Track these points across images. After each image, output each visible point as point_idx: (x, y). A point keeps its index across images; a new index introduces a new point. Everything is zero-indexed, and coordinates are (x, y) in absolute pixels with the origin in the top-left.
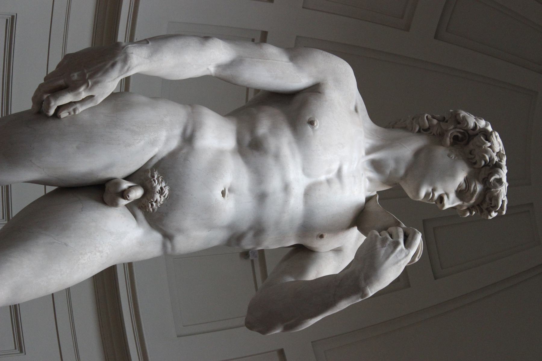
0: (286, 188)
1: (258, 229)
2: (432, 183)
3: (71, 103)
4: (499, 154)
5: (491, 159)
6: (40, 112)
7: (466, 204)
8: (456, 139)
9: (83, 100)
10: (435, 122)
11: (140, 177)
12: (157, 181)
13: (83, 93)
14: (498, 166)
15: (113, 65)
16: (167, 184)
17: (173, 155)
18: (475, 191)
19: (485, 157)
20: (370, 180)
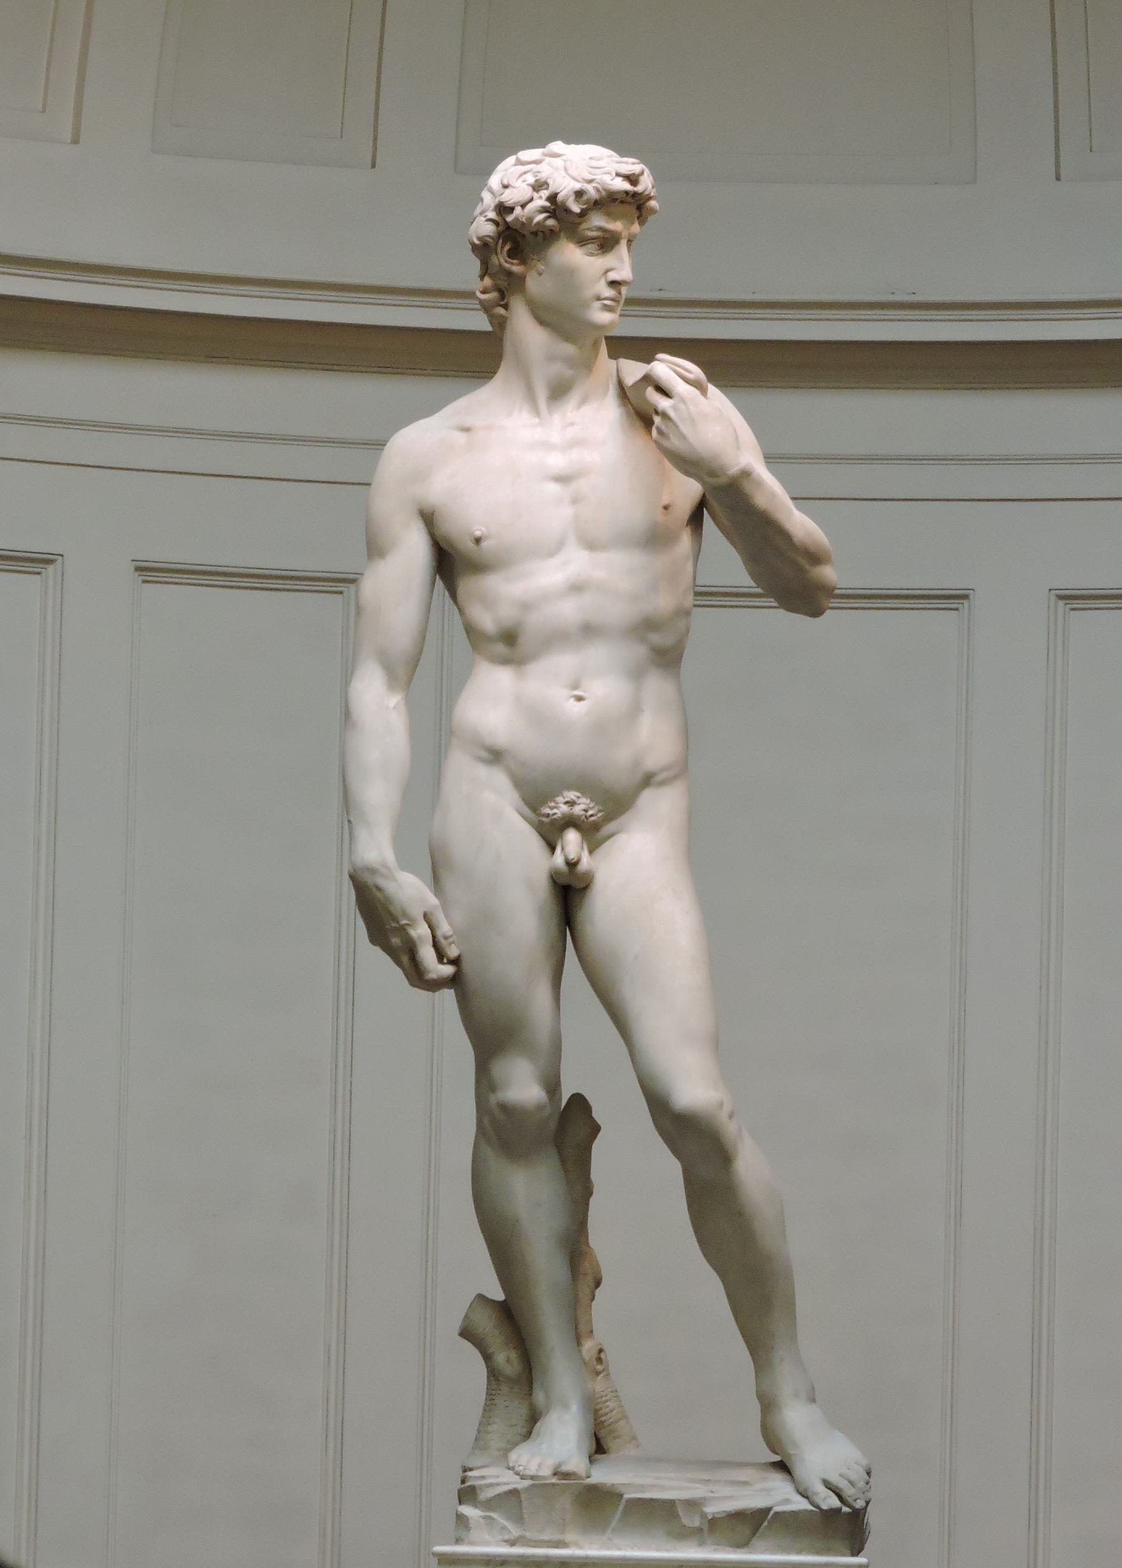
0: (576, 588)
1: (644, 627)
2: (586, 305)
3: (436, 945)
4: (539, 186)
5: (544, 210)
6: (454, 981)
7: (625, 234)
8: (516, 253)
9: (431, 927)
10: (488, 281)
11: (550, 834)
12: (555, 811)
13: (420, 931)
14: (552, 198)
15: (379, 889)
16: (559, 793)
17: (519, 783)
18: (600, 229)
19: (538, 223)
20: (584, 401)
